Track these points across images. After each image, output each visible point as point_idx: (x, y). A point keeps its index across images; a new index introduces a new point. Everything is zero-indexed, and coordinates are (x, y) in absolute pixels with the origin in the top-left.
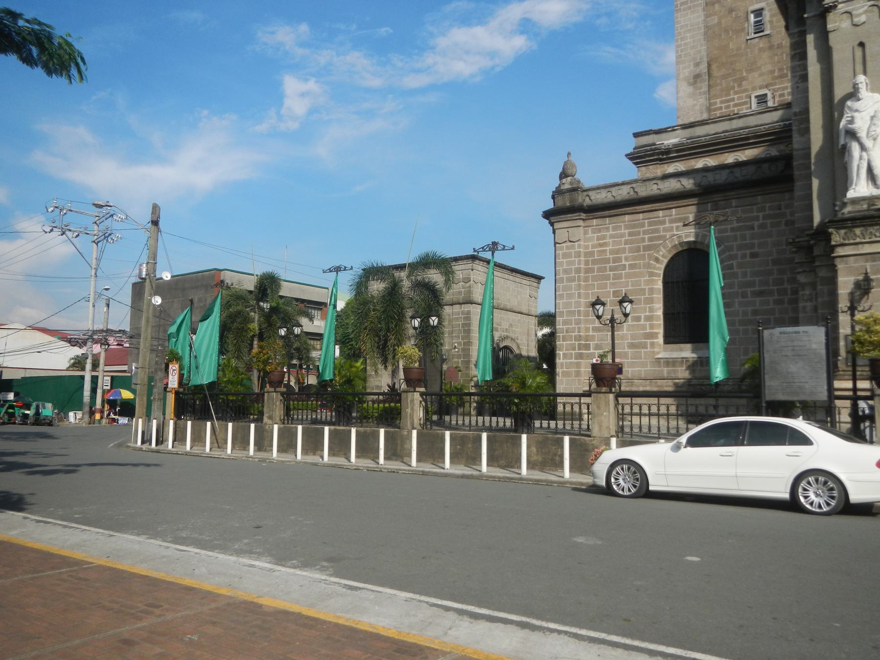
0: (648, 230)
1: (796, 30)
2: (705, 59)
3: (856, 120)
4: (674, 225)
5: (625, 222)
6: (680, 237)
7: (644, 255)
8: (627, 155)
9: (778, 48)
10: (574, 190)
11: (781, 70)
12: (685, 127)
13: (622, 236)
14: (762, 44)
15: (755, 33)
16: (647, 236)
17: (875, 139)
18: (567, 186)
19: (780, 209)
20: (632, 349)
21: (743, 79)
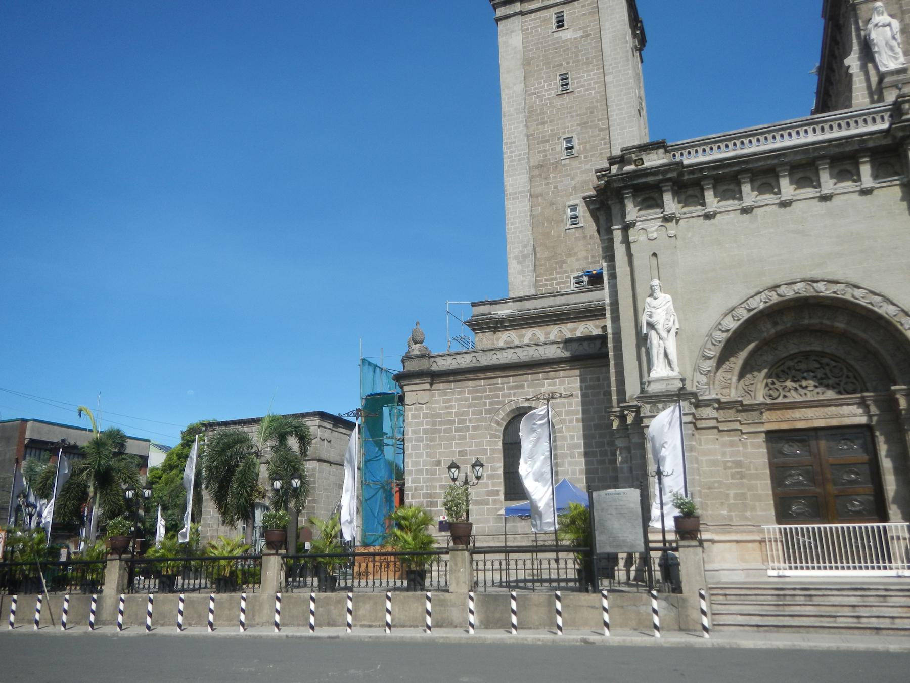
0: (488, 395)
1: (606, 237)
2: (532, 242)
3: (654, 315)
4: (512, 391)
5: (468, 387)
6: (517, 402)
7: (486, 418)
8: (465, 323)
9: (590, 238)
10: (422, 356)
11: (593, 257)
12: (517, 300)
13: (466, 399)
14: (578, 233)
15: (572, 224)
16: (488, 401)
17: (669, 331)
18: (416, 352)
19: (599, 381)
20: (476, 506)
21: (563, 262)
